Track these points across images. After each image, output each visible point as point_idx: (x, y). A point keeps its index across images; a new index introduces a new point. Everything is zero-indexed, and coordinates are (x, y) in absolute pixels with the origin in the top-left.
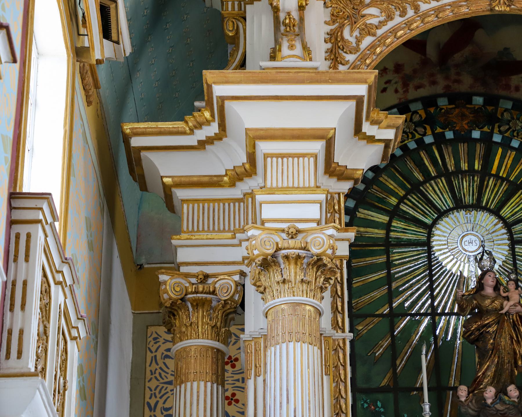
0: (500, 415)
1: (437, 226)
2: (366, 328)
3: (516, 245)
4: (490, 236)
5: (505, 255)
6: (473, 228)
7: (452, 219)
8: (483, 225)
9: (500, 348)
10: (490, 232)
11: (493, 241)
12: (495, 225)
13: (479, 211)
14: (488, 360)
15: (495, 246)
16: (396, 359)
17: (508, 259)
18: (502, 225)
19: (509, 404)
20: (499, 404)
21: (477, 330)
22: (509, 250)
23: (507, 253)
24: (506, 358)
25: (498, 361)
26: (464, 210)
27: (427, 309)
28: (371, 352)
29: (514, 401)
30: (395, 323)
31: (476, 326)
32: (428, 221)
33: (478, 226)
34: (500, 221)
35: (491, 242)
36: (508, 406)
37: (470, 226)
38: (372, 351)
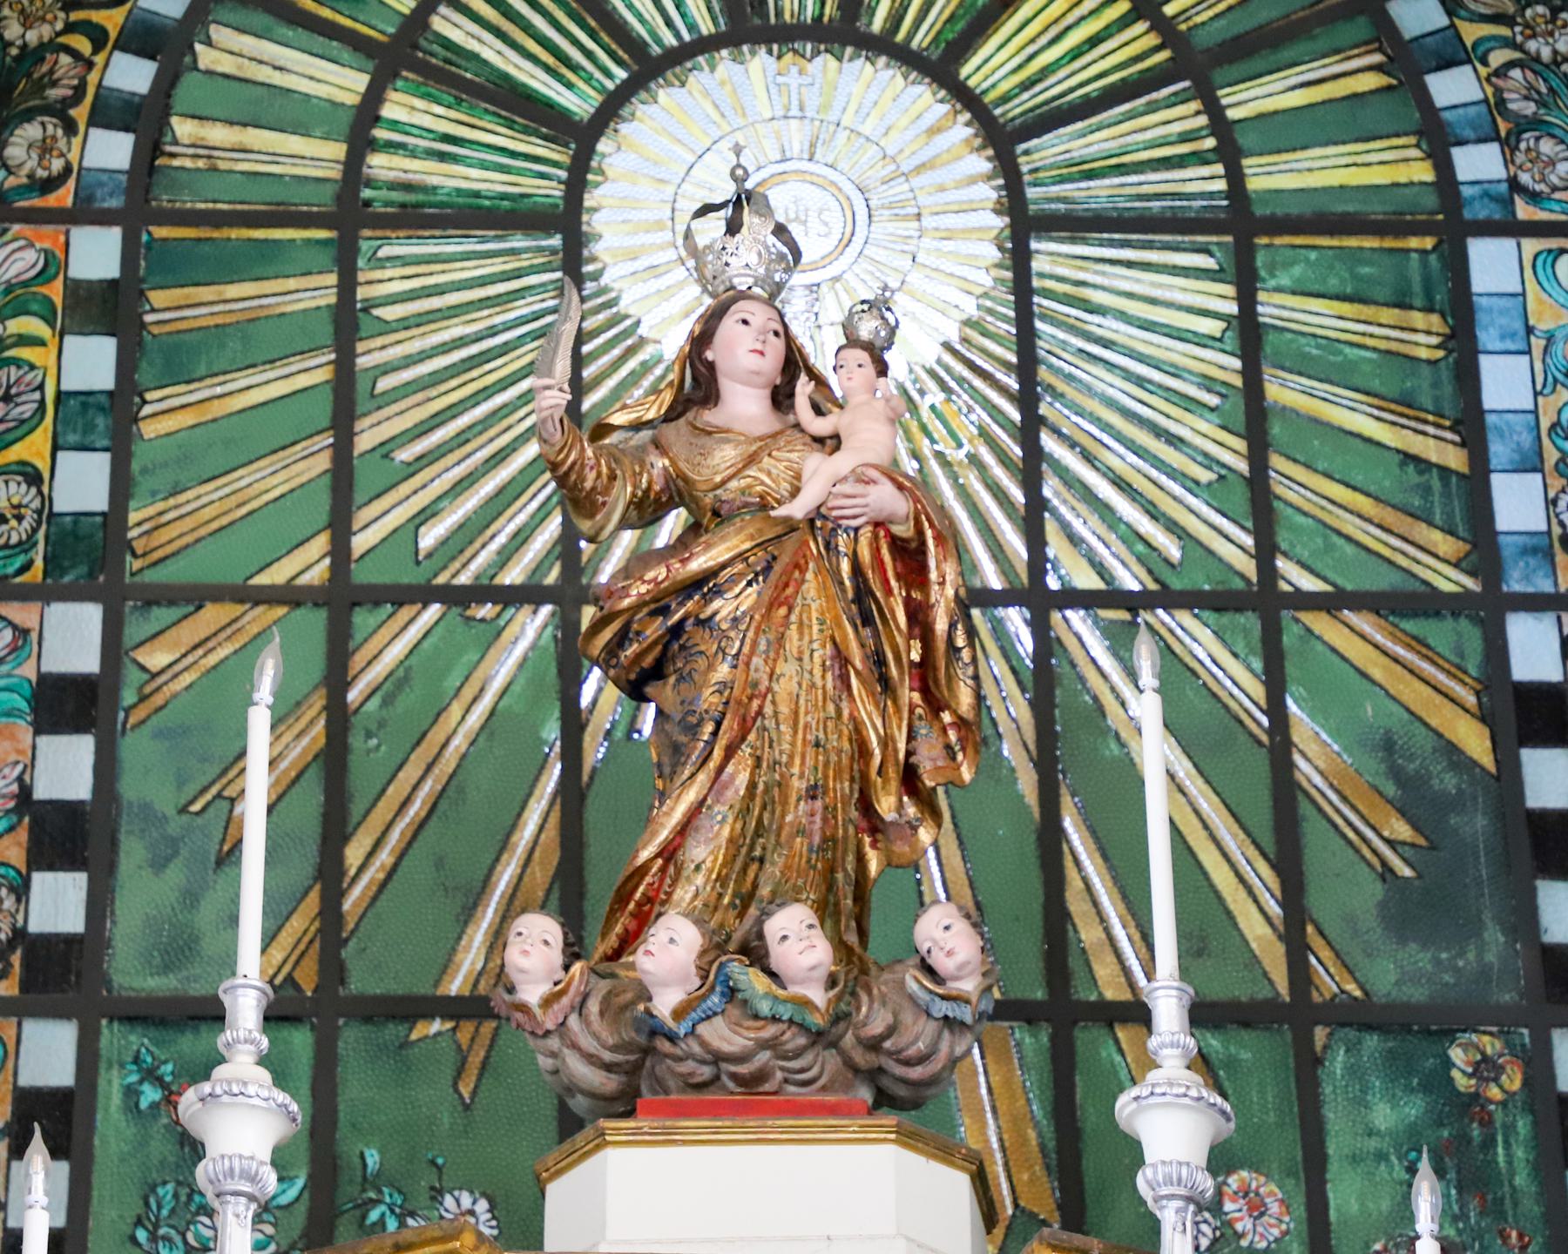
0: (731, 1085)
1: (624, 128)
2: (190, 659)
3: (1039, 239)
4: (901, 187)
5: (979, 291)
6: (813, 145)
7: (706, 93)
8: (866, 129)
9: (768, 710)
10: (905, 168)
11: (918, 216)
12: (934, 131)
13: (851, 60)
14: (693, 775)
15: (926, 242)
16: (346, 839)
17: (990, 311)
18: (970, 131)
19: (775, 1019)
20: (718, 1021)
21: (654, 614)
22: (998, 266)
23: (987, 281)
24: (796, 770)
25: (752, 786)
26: (770, 52)
27: (540, 567)
28: (208, 796)
29: (806, 1003)
30: (359, 637)
31: (643, 589)
32: (579, 102)
33: (842, 135)
34: (956, 112)
35: (906, 218)
36: (770, 1031)
37: (796, 136)
38: (214, 790)
